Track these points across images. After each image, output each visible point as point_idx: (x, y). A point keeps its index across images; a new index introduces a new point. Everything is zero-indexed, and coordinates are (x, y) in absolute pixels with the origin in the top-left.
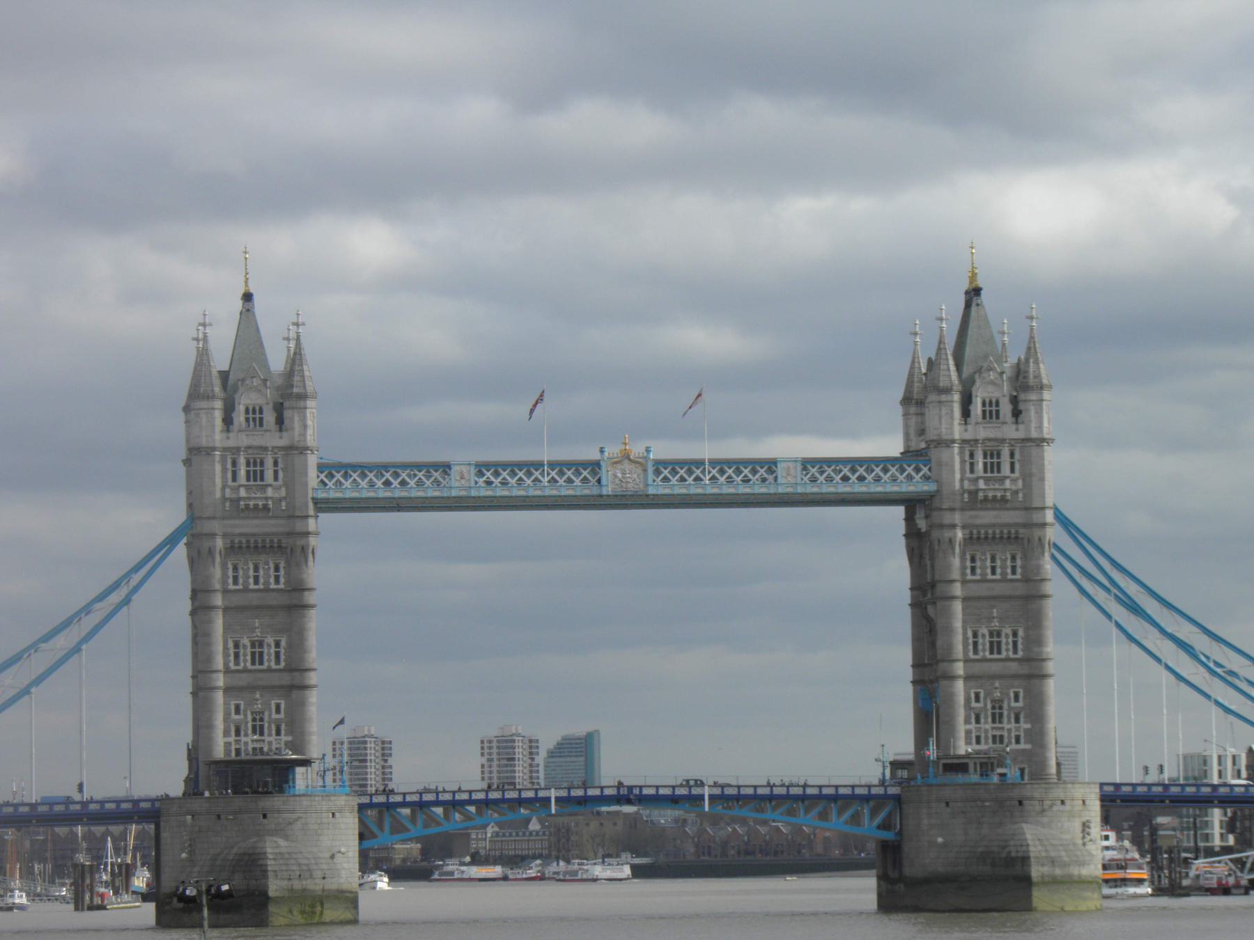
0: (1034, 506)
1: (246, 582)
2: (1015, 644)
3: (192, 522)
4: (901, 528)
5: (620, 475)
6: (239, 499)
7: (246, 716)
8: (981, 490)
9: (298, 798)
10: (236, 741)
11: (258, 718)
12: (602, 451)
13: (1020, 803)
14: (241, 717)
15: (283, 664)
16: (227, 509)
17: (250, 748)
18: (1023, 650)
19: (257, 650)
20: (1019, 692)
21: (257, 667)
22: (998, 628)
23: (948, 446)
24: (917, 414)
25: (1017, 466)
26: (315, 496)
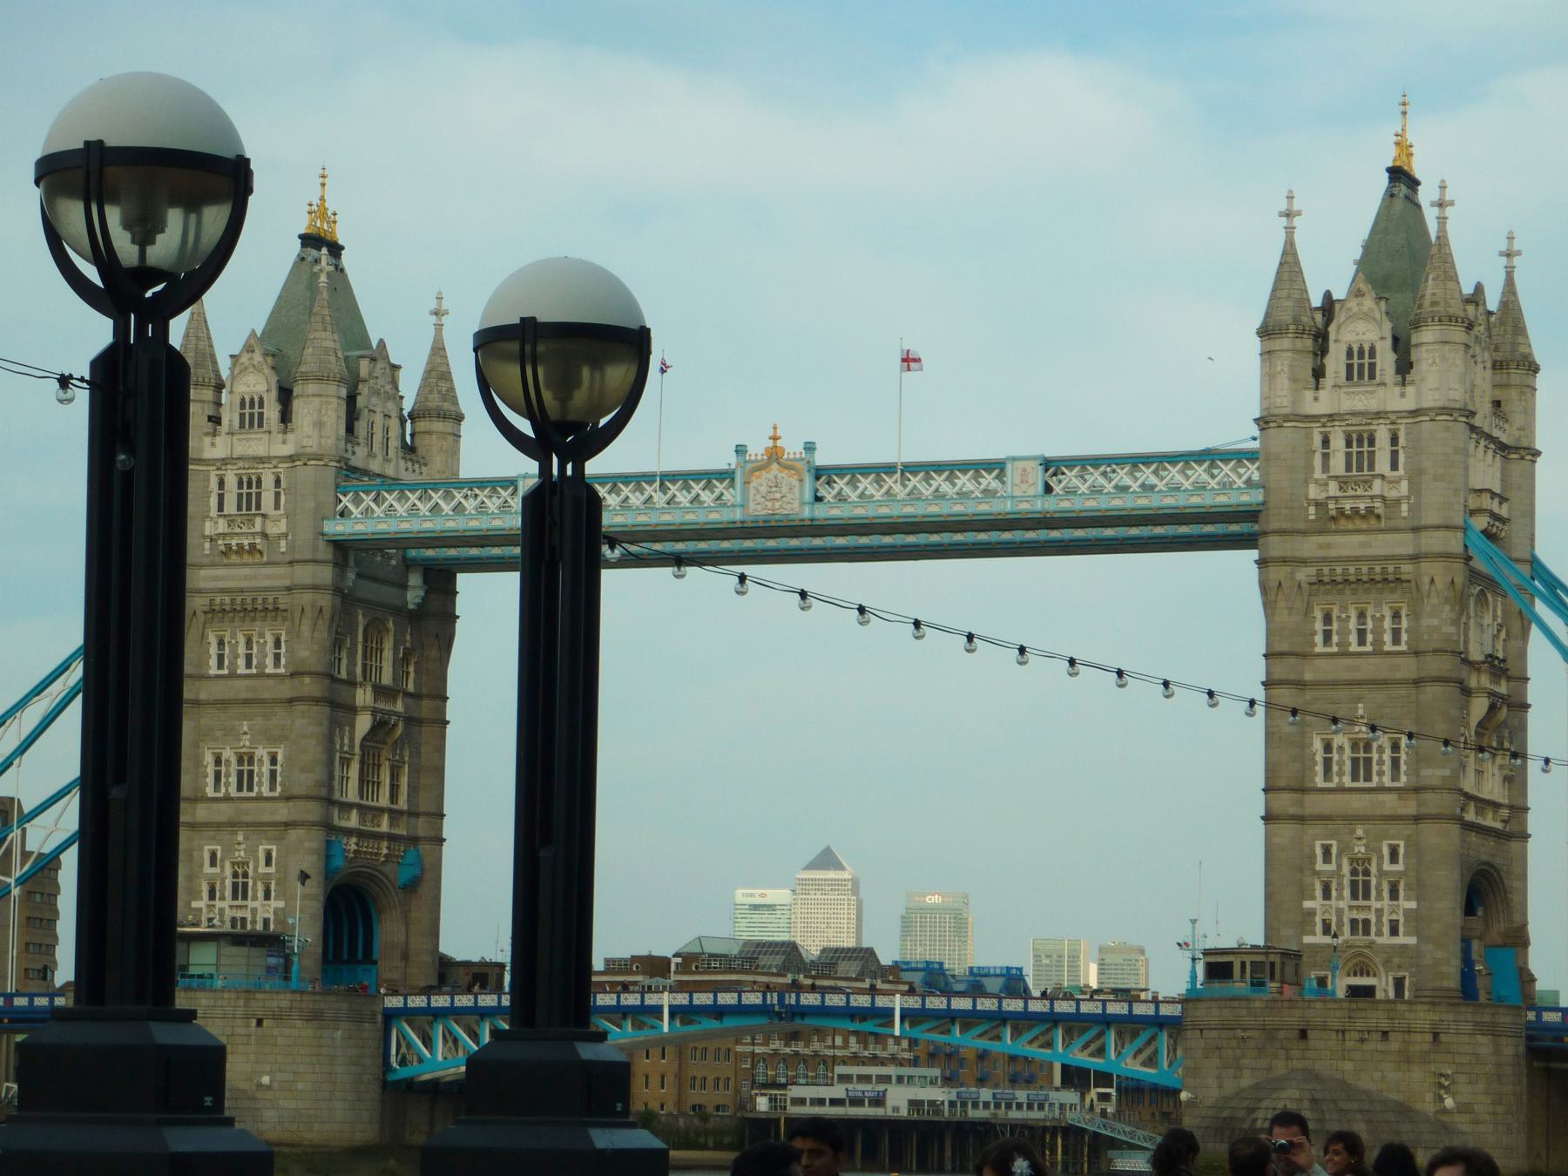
1: (233, 665)
2: (1395, 763)
7: (222, 867)
8: (1328, 498)
9: (192, 994)
10: (208, 906)
12: (740, 450)
13: (1303, 1034)
14: (217, 870)
16: (207, 552)
17: (227, 919)
18: (1407, 775)
19: (246, 768)
20: (1398, 845)
22: (1365, 736)
25: (1402, 458)
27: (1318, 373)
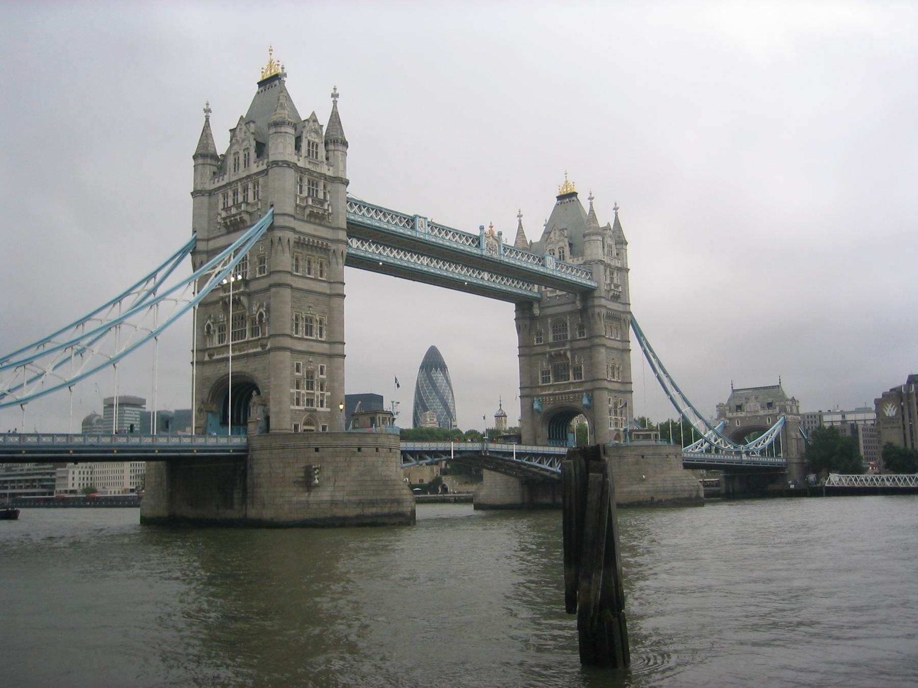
3: (273, 218)
4: (514, 315)
11: (310, 375)
12: (482, 228)
13: (676, 457)
15: (325, 337)
19: (309, 324)
27: (603, 248)
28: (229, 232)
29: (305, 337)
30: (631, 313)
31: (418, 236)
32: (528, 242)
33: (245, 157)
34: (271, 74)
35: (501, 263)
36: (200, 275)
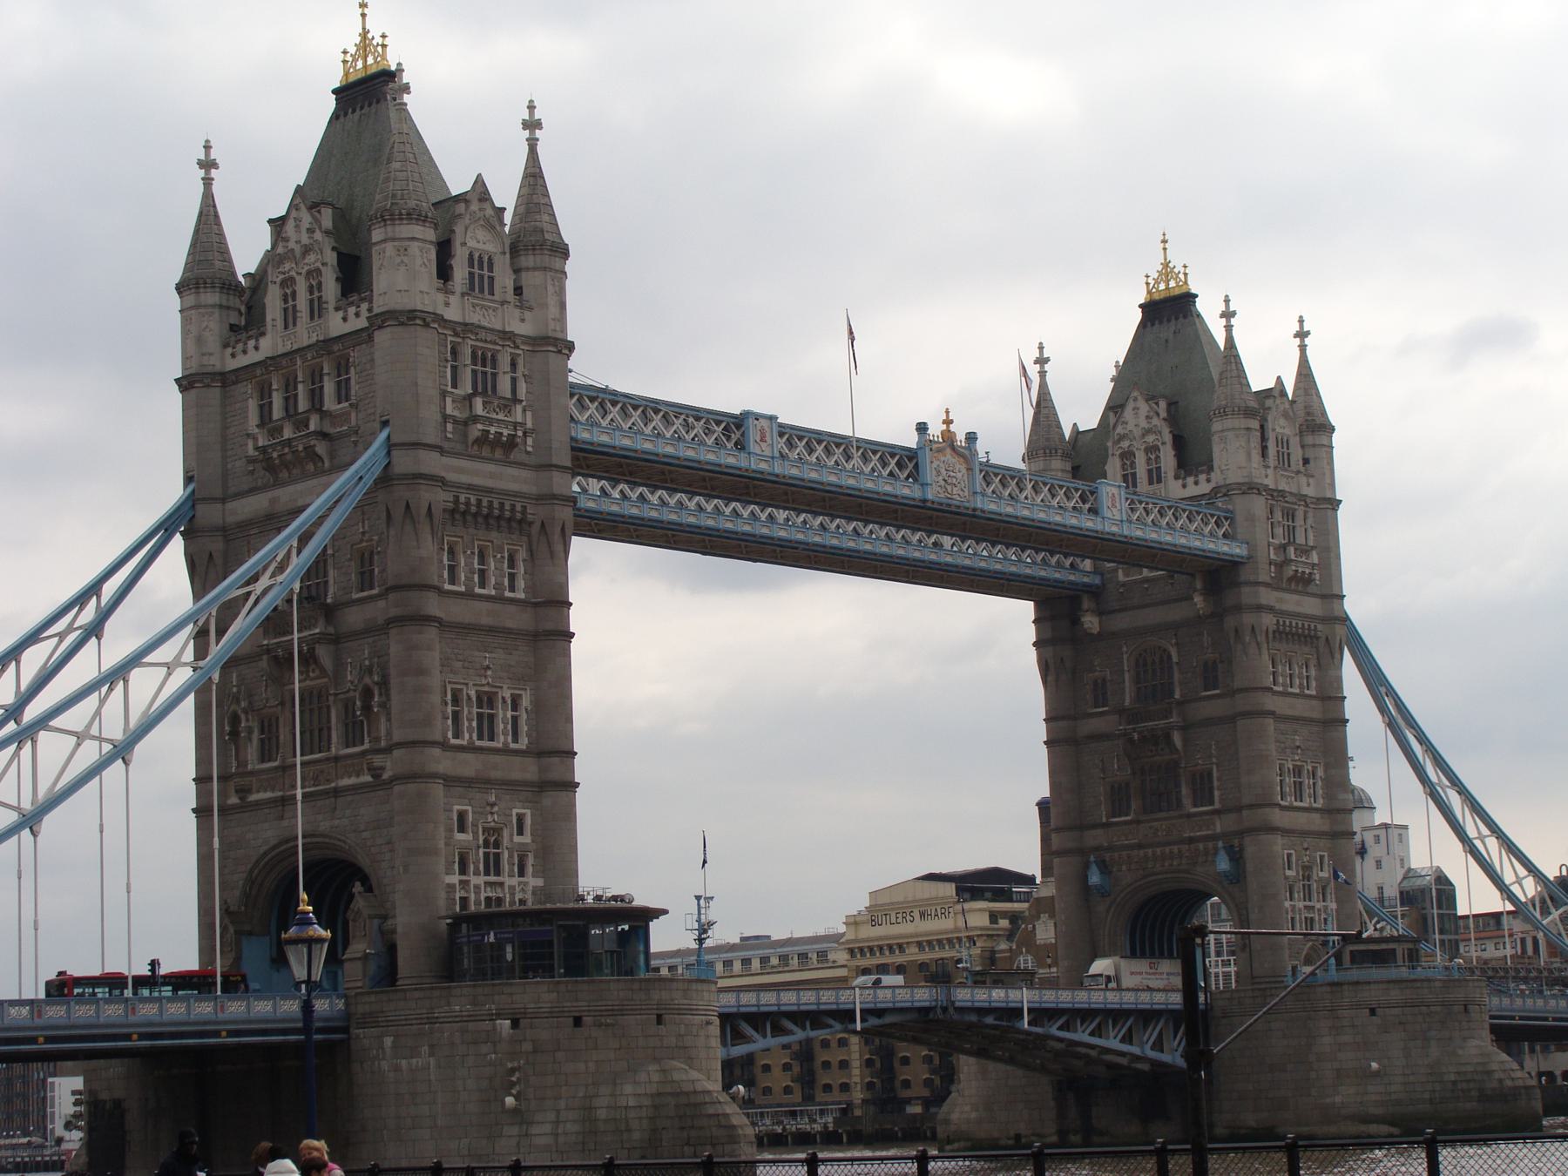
0: (1335, 592)
2: (1314, 784)
3: (389, 453)
4: (1030, 633)
5: (943, 471)
6: (475, 419)
10: (461, 882)
11: (493, 838)
12: (922, 428)
13: (1466, 1010)
15: (523, 743)
16: (449, 436)
21: (485, 743)
23: (1260, 494)
24: (1063, 471)
26: (573, 434)
27: (1264, 454)
28: (278, 484)
29: (478, 743)
30: (1345, 619)
31: (753, 466)
32: (1067, 433)
33: (311, 293)
34: (365, 66)
35: (974, 516)
36: (220, 602)
